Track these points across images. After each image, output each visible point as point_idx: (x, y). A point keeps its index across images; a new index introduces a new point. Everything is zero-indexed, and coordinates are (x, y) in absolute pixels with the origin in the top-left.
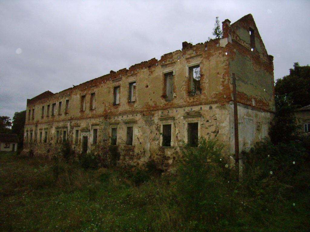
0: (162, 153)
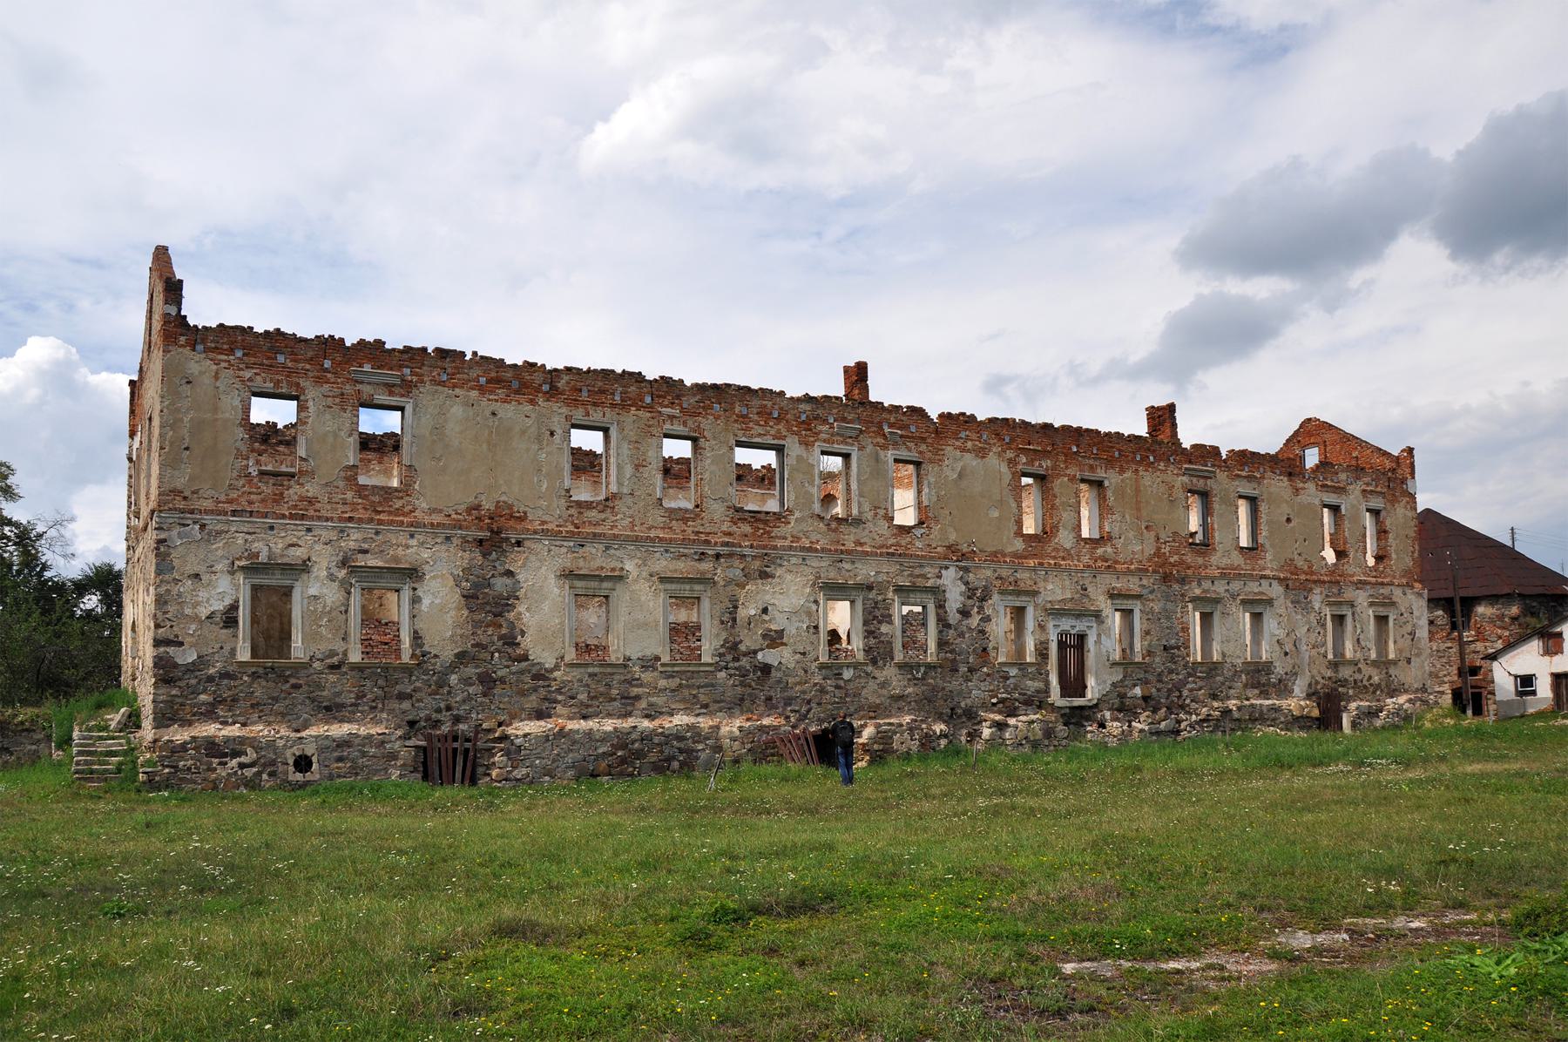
0: (1333, 675)
